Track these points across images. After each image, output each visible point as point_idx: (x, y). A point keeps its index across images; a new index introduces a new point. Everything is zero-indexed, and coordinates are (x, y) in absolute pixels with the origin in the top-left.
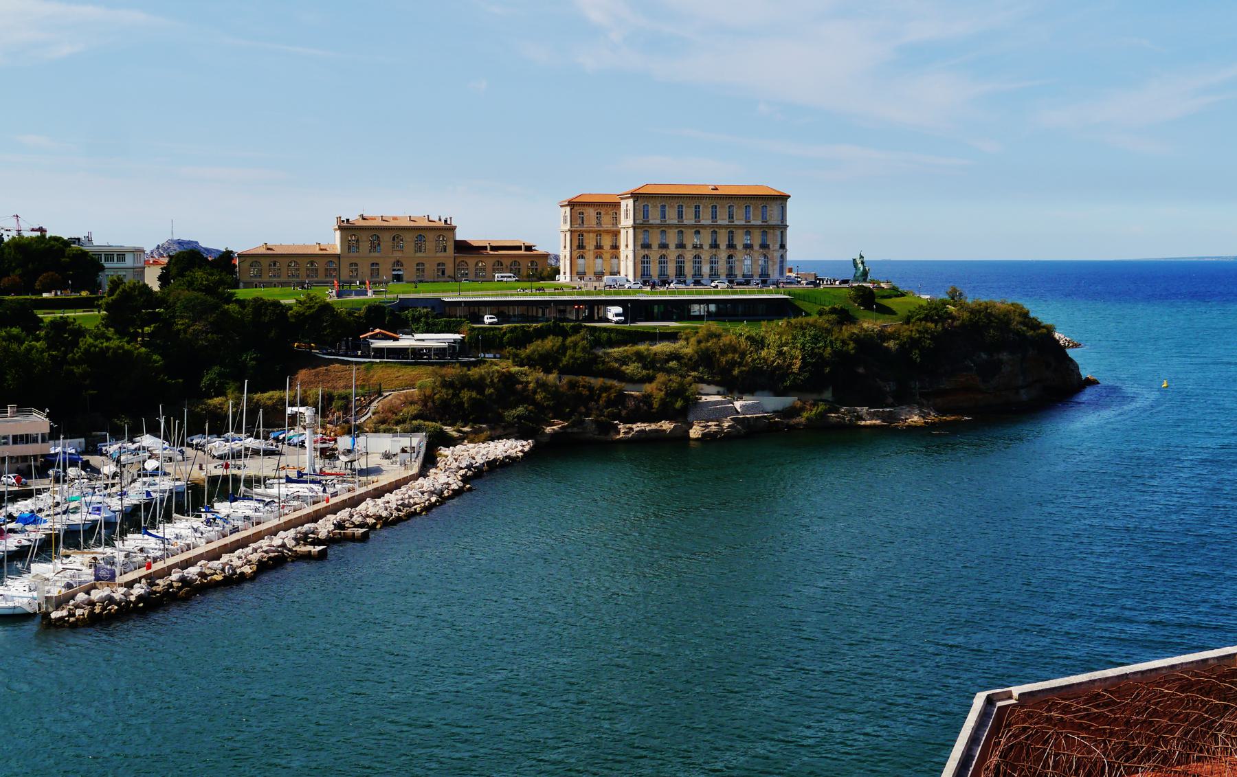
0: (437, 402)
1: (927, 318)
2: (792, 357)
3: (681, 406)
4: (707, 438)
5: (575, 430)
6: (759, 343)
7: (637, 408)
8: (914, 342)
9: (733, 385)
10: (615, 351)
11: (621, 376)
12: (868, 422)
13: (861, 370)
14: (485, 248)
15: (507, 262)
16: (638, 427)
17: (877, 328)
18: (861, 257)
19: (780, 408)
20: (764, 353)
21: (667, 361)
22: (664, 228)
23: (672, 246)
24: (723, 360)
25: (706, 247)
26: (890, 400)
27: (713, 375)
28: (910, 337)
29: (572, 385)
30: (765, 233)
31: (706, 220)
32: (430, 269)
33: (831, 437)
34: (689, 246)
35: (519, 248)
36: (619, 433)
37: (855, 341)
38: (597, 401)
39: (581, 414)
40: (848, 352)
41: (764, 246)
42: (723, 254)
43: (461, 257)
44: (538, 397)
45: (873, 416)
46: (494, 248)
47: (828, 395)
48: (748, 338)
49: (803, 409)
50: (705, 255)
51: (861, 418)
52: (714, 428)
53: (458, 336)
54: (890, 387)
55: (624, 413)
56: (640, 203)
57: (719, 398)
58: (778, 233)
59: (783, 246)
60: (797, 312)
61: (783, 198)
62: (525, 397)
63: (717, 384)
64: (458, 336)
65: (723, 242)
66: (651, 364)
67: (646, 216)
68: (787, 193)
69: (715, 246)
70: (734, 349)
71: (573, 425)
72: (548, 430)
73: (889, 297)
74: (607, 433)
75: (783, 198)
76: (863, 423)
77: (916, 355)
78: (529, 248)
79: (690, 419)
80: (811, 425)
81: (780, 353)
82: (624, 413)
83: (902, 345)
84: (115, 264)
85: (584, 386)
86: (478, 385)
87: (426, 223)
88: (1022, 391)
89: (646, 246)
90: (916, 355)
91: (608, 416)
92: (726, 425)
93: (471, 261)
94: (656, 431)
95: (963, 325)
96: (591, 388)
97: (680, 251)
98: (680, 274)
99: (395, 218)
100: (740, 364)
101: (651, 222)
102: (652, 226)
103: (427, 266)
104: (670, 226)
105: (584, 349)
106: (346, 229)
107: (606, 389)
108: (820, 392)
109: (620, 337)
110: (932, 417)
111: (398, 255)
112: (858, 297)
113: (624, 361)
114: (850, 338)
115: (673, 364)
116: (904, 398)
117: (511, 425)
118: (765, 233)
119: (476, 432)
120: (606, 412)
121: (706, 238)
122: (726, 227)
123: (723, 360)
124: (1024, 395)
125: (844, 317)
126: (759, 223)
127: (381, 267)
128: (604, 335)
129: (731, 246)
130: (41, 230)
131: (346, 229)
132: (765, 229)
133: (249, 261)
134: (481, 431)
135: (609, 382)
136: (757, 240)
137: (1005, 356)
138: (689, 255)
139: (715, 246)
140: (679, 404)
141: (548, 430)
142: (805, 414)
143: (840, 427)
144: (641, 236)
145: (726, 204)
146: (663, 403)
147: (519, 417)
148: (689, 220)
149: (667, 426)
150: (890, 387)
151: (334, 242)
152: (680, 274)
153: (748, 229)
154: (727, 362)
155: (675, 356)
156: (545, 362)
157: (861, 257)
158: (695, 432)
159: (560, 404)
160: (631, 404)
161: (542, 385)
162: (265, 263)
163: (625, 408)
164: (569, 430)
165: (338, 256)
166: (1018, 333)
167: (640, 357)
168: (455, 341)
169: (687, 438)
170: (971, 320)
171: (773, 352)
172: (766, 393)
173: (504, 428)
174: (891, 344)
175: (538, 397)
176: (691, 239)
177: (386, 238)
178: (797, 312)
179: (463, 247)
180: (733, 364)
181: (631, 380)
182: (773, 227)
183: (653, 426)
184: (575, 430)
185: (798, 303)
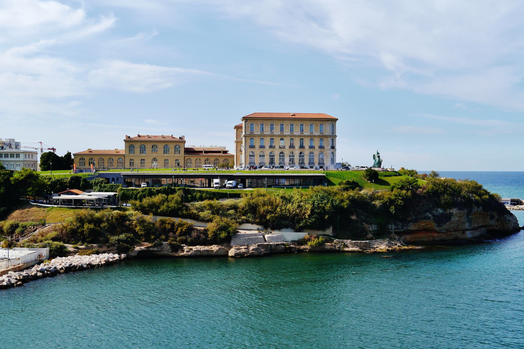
0: (68, 230)
1: (402, 188)
2: (306, 209)
3: (226, 236)
4: (239, 257)
5: (155, 249)
6: (287, 200)
7: (198, 237)
8: (392, 202)
9: (267, 225)
10: (198, 204)
11: (196, 218)
12: (350, 249)
13: (354, 217)
14: (202, 152)
15: (212, 159)
16: (199, 247)
17: (370, 193)
18: (378, 153)
19: (296, 239)
20: (289, 206)
21: (228, 210)
22: (262, 137)
23: (267, 147)
24: (262, 210)
25: (287, 147)
26: (370, 235)
27: (255, 218)
28: (389, 199)
29: (163, 222)
30: (322, 140)
31: (287, 132)
32: (172, 162)
33: (325, 259)
34: (277, 147)
35: (220, 152)
36: (184, 251)
37: (350, 200)
38: (175, 233)
39: (161, 240)
40: (342, 207)
41: (321, 147)
42: (297, 152)
43: (188, 156)
44: (137, 229)
45: (355, 245)
46: (206, 152)
47: (329, 232)
48: (282, 197)
49: (309, 240)
50: (287, 152)
51: (347, 246)
52: (243, 250)
53: (112, 194)
54: (373, 228)
55: (189, 239)
56: (249, 123)
57: (256, 232)
58: (330, 140)
59: (333, 147)
60: (330, 184)
61: (335, 120)
62: (129, 229)
63: (257, 224)
64: (112, 194)
65: (297, 144)
66: (216, 211)
67: (252, 130)
68: (334, 116)
69: (292, 146)
70: (271, 203)
71: (155, 246)
72: (137, 248)
73: (390, 176)
74: (176, 251)
75: (335, 120)
76: (346, 249)
77: (392, 209)
78: (225, 152)
79: (232, 244)
80: (313, 251)
81: (299, 206)
82: (189, 239)
83: (384, 204)
84: (15, 159)
85: (169, 223)
86: (98, 221)
87: (171, 139)
88: (468, 232)
89: (252, 147)
90: (392, 209)
91: (179, 241)
92: (251, 248)
93: (193, 158)
94: (207, 251)
95: (428, 193)
96: (173, 225)
97: (272, 150)
98: (272, 162)
99: (155, 136)
100: (271, 212)
101: (255, 133)
102: (255, 136)
103: (170, 161)
104: (266, 136)
105: (176, 202)
106: (129, 141)
107: (180, 225)
108: (324, 229)
109: (208, 195)
110: (397, 246)
111: (154, 155)
112: (367, 175)
113: (202, 209)
114: (348, 198)
115: (231, 212)
116: (379, 235)
117: (113, 245)
118: (322, 140)
119: (87, 248)
120: (178, 239)
121: (286, 143)
122: (299, 136)
123: (262, 210)
124: (469, 235)
125: (353, 185)
126: (319, 134)
127: (146, 161)
128: (199, 194)
129: (302, 147)
130: (53, 149)
131: (129, 141)
132: (322, 137)
133: (79, 157)
134: (92, 247)
135: (185, 221)
136: (317, 143)
137: (454, 211)
138: (277, 152)
139: (292, 146)
140: (223, 235)
141: (137, 248)
142: (309, 243)
143: (332, 251)
144: (249, 141)
145: (299, 123)
146: (215, 234)
147: (119, 241)
148: (277, 131)
149: (215, 248)
150: (373, 228)
151: (121, 147)
152: (272, 162)
153: (312, 137)
154: (264, 211)
155: (235, 207)
156: (152, 209)
157: (378, 153)
158: (232, 252)
159: (150, 233)
160: (194, 234)
161: (142, 222)
162: (87, 159)
163: (190, 236)
164: (151, 249)
165: (124, 156)
166: (464, 197)
167: (211, 207)
168: (109, 197)
169: (227, 256)
170: (432, 189)
171: (295, 205)
172: (289, 230)
173: (108, 247)
174: (377, 203)
175: (137, 229)
176: (278, 143)
177: (149, 146)
178: (330, 184)
179: (190, 151)
180: (268, 212)
181: (203, 220)
182: (326, 137)
183: (206, 248)
184: (155, 249)
185: (331, 179)
